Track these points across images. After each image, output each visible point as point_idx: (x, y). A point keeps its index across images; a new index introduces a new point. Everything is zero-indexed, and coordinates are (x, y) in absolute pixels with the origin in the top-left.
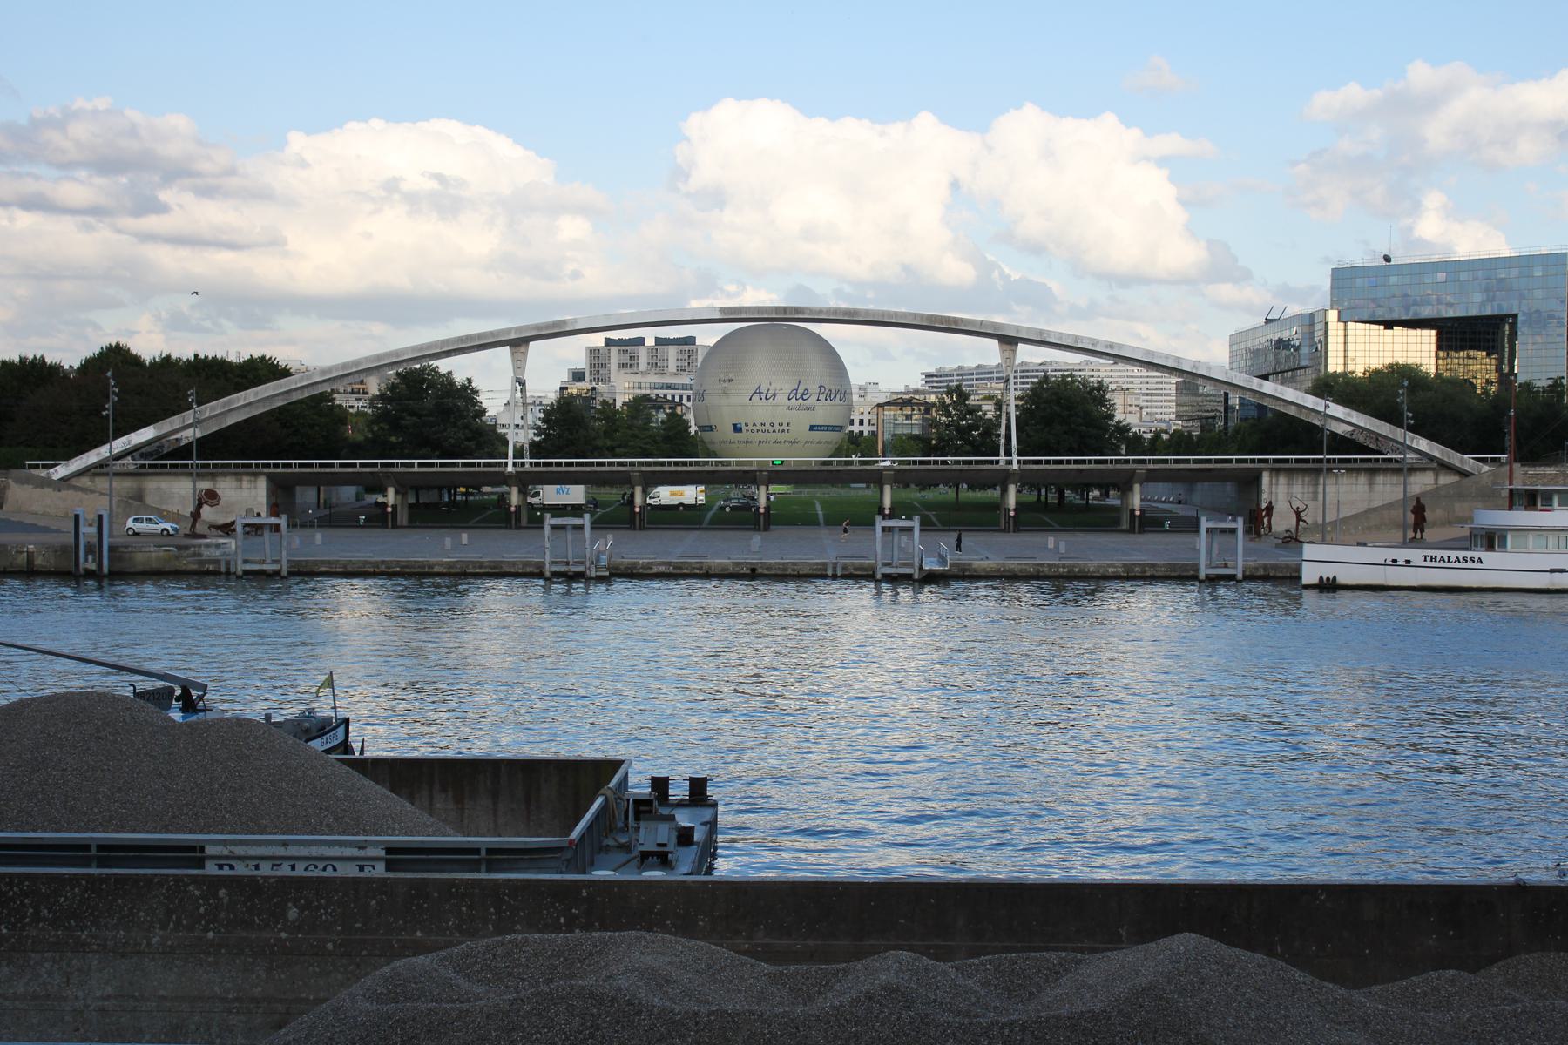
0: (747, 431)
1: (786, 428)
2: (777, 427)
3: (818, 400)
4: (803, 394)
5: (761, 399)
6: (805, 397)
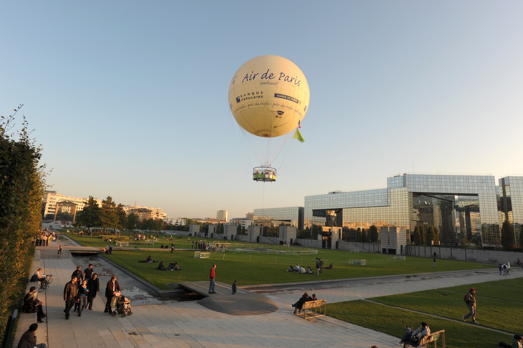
0: (242, 100)
2: (256, 95)
3: (279, 79)
4: (270, 76)
5: (247, 80)
6: (271, 77)
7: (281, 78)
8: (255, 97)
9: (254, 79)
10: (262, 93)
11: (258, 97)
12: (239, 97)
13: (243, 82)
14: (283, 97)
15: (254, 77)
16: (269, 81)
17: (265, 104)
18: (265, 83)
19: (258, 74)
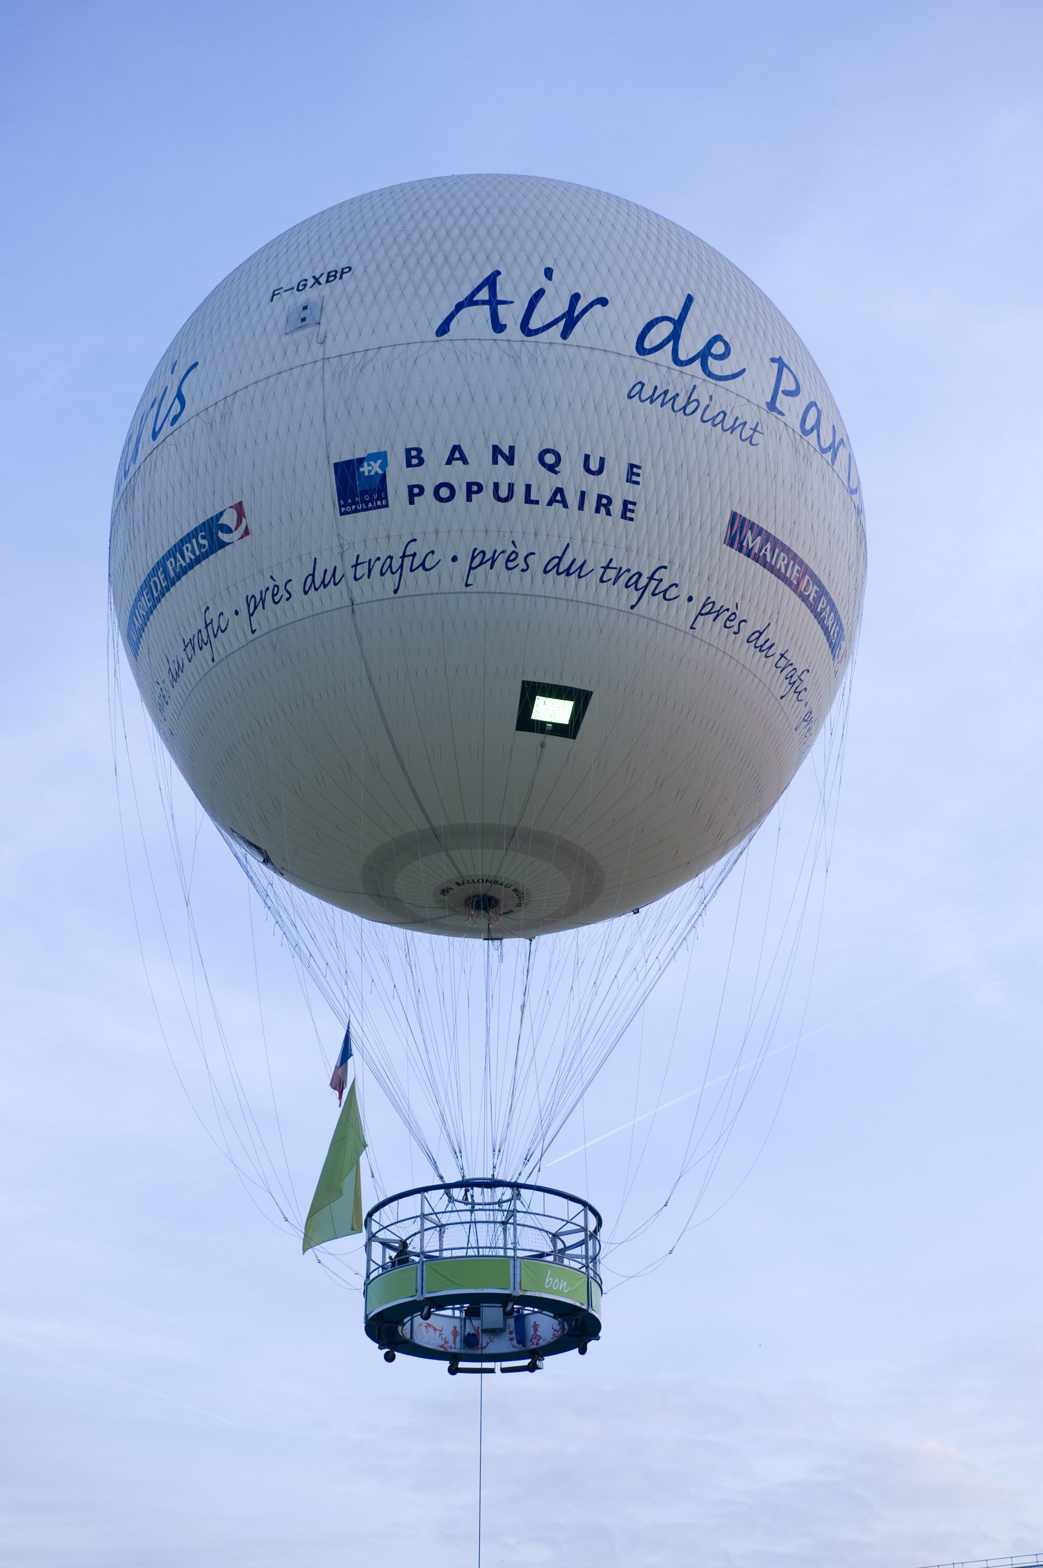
0: (414, 492)
1: (618, 490)
5: (498, 327)
7: (782, 401)
8: (559, 491)
9: (565, 335)
10: (632, 472)
11: (591, 502)
12: (382, 456)
13: (443, 329)
14: (781, 564)
15: (570, 320)
16: (702, 394)
17: (643, 582)
18: (662, 397)
19: (603, 302)
